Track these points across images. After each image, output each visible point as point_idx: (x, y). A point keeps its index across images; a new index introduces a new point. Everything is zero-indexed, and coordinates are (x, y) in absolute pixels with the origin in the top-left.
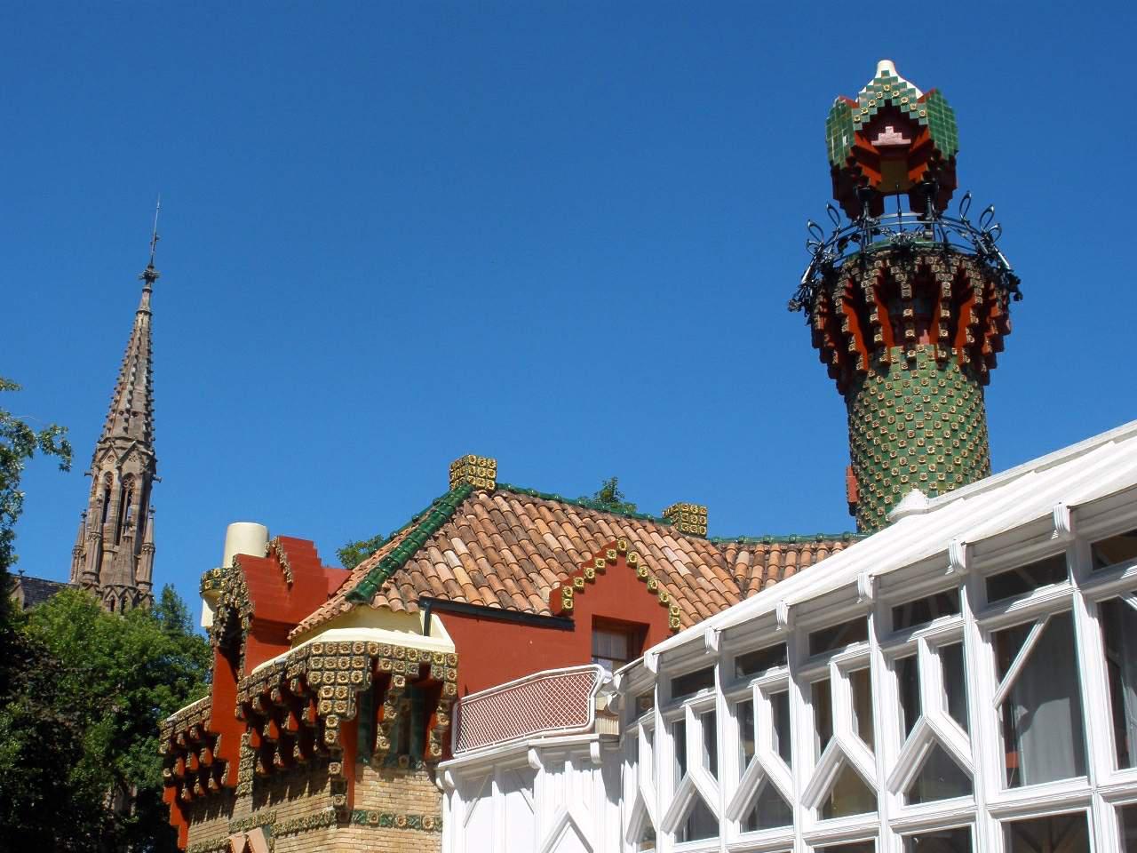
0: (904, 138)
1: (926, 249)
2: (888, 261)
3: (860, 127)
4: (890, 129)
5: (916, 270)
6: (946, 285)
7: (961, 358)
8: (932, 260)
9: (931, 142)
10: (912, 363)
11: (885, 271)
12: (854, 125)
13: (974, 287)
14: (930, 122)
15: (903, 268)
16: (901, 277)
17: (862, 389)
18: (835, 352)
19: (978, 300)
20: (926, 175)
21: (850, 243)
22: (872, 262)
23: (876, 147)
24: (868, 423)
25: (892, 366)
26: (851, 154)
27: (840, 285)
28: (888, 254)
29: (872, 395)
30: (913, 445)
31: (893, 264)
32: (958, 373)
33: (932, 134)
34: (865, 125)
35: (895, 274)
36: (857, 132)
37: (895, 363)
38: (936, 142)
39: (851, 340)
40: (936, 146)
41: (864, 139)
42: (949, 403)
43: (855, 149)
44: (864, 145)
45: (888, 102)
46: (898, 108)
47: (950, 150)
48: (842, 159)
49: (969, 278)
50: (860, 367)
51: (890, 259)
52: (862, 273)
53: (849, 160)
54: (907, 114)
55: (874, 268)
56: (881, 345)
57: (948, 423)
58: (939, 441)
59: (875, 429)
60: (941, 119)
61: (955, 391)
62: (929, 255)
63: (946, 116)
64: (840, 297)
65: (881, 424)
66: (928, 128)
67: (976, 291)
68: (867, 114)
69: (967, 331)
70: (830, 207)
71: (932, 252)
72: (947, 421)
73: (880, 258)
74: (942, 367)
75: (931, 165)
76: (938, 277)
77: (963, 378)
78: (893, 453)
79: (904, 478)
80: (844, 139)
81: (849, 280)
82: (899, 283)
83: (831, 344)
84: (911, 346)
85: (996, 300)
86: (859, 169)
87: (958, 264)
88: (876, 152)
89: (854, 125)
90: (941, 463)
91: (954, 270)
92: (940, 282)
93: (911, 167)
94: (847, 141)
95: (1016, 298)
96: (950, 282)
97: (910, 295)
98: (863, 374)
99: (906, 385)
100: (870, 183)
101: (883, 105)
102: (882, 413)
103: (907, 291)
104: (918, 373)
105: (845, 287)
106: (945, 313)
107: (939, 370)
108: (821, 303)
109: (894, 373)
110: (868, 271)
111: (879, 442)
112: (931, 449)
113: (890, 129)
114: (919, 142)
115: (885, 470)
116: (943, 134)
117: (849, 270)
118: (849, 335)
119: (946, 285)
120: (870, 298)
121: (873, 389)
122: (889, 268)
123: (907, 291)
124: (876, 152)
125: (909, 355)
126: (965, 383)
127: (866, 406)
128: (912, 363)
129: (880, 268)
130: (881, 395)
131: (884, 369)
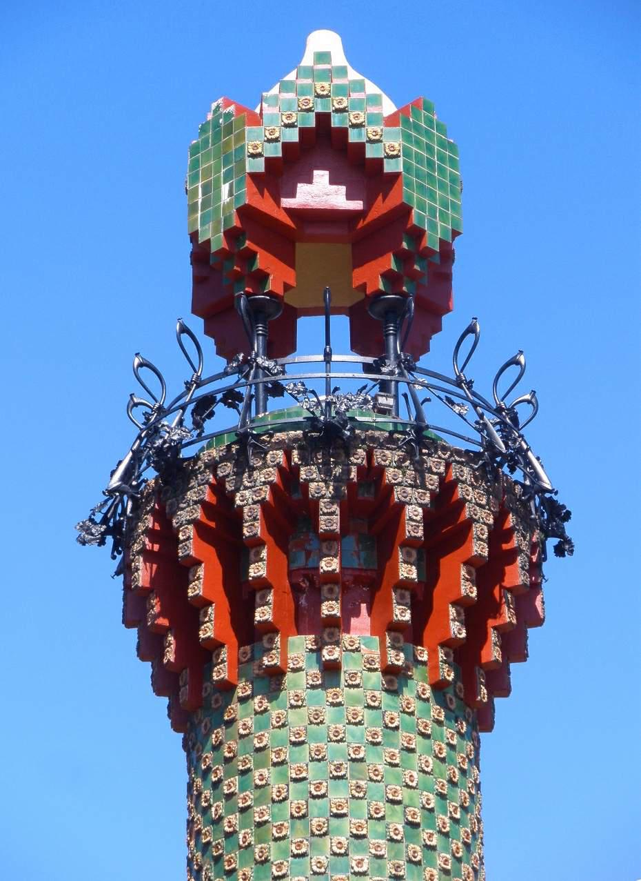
0: (350, 197)
1: (377, 434)
2: (295, 452)
3: (259, 166)
4: (321, 177)
5: (353, 475)
6: (414, 512)
7: (435, 668)
8: (388, 457)
9: (405, 210)
10: (331, 671)
11: (289, 474)
12: (248, 161)
13: (470, 522)
14: (407, 168)
15: (326, 470)
16: (319, 487)
18: (171, 639)
19: (479, 548)
20: (388, 276)
21: (220, 408)
22: (261, 452)
23: (290, 212)
24: (229, 796)
25: (289, 676)
26: (235, 222)
27: (191, 495)
28: (296, 440)
29: (242, 736)
30: (321, 853)
31: (305, 461)
32: (427, 700)
33: (410, 193)
35: (308, 481)
36: (254, 176)
38: (415, 210)
39: (206, 614)
40: (414, 220)
41: (266, 193)
42: (406, 765)
43: (246, 212)
44: (265, 205)
47: (444, 228)
48: (216, 231)
49: (463, 502)
50: (221, 673)
51: (300, 448)
52: (239, 474)
53: (232, 235)
54: (361, 147)
55: (265, 466)
56: (270, 629)
58: (378, 847)
59: (243, 810)
60: (430, 164)
61: (420, 738)
62: (382, 446)
63: (441, 159)
64: (189, 522)
65: (258, 801)
66: (403, 179)
67: (476, 529)
68: (276, 140)
69: (452, 612)
70: (184, 329)
73: (279, 445)
74: (396, 687)
75: (403, 258)
76: (397, 494)
77: (436, 711)
78: (279, 866)
80: (225, 188)
81: (211, 486)
82: (316, 502)
83: (164, 622)
84: (331, 635)
85: (516, 552)
86: (251, 256)
87: (442, 469)
88: (288, 221)
89: (248, 161)
91: (433, 481)
92: (401, 506)
93: (359, 261)
94: (231, 194)
95: (559, 551)
96: (420, 505)
97: (336, 527)
98: (227, 688)
100: (270, 287)
101: (312, 123)
102: (262, 777)
103: (330, 519)
104: (344, 694)
105: (202, 503)
106: (407, 572)
107: (386, 691)
108: (148, 532)
109: (292, 692)
110: (252, 469)
111: (251, 839)
112: (360, 863)
113: (321, 177)
114: (381, 207)
116: (432, 196)
117: (213, 466)
119: (414, 512)
120: (253, 527)
122: (297, 468)
123: (330, 519)
124: (288, 221)
125: (326, 655)
126: (439, 723)
127: (228, 760)
128: (331, 671)
129: (278, 466)
130: (260, 738)
131: (272, 680)
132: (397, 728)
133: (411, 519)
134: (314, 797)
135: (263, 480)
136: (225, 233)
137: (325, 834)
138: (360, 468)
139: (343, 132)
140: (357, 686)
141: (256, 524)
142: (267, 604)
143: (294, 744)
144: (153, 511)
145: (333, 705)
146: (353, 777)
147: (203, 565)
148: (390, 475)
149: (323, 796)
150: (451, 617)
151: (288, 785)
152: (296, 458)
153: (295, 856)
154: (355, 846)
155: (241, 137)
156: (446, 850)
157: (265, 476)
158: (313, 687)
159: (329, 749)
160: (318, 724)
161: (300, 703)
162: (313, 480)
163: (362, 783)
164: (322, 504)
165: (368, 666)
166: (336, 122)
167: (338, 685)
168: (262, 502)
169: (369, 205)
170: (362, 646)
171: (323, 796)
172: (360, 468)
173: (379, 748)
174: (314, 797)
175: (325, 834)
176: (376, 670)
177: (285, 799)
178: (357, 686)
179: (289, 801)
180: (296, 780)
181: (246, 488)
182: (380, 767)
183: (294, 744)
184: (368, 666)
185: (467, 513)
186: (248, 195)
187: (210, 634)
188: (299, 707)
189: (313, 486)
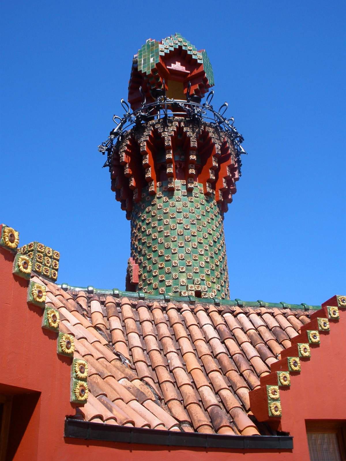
0: (186, 70)
3: (163, 54)
7: (218, 196)
8: (211, 130)
9: (203, 73)
10: (190, 191)
11: (180, 129)
17: (150, 205)
18: (133, 179)
22: (171, 122)
23: (169, 69)
24: (154, 228)
25: (176, 191)
26: (155, 67)
27: (145, 134)
28: (182, 120)
29: (158, 209)
30: (189, 247)
31: (186, 126)
35: (187, 132)
36: (161, 56)
37: (178, 190)
43: (158, 65)
44: (164, 65)
45: (180, 47)
46: (186, 51)
48: (149, 69)
53: (153, 70)
54: (191, 56)
55: (172, 126)
56: (171, 175)
59: (160, 232)
64: (144, 141)
65: (165, 229)
69: (224, 180)
71: (210, 126)
73: (177, 120)
78: (175, 250)
79: (182, 268)
80: (152, 60)
81: (152, 131)
84: (191, 180)
88: (167, 70)
92: (214, 144)
99: (185, 206)
103: (194, 144)
105: (149, 135)
106: (214, 164)
107: (206, 200)
108: (127, 145)
109: (158, 205)
110: (168, 126)
114: (196, 72)
115: (167, 261)
118: (147, 166)
120: (168, 143)
121: (159, 203)
122: (183, 127)
125: (189, 186)
127: (153, 216)
128: (190, 191)
129: (176, 126)
130: (166, 210)
131: (170, 192)
134: (186, 229)
135: (171, 130)
136: (151, 70)
137: (190, 241)
140: (197, 197)
141: (170, 142)
142: (171, 167)
143: (178, 212)
144: (129, 139)
145: (190, 202)
146: (198, 225)
147: (148, 155)
148: (210, 134)
149: (188, 229)
150: (224, 182)
151: (176, 225)
152: (182, 124)
153: (180, 247)
154: (199, 246)
155: (158, 46)
157: (172, 129)
158: (184, 196)
159: (189, 215)
160: (186, 207)
161: (180, 200)
162: (188, 132)
163: (201, 227)
164: (191, 138)
165: (200, 192)
166: (184, 48)
167: (192, 196)
168: (171, 136)
170: (198, 186)
171: (188, 229)
173: (205, 217)
174: (186, 229)
175: (190, 241)
176: (202, 193)
177: (176, 229)
178: (197, 197)
179: (177, 230)
180: (179, 223)
181: (166, 132)
182: (205, 223)
183: (178, 212)
184: (200, 192)
186: (159, 60)
187: (150, 176)
188: (180, 201)
189: (188, 133)
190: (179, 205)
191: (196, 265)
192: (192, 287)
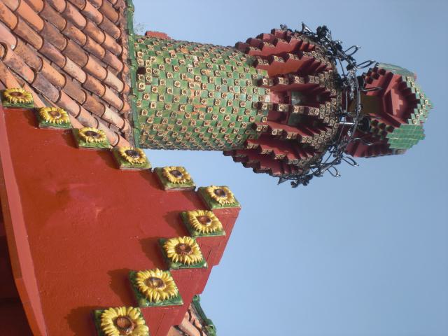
0: (397, 110)
3: (404, 80)
4: (401, 102)
9: (398, 125)
10: (259, 83)
11: (324, 69)
16: (324, 77)
20: (375, 123)
26: (387, 72)
34: (405, 84)
35: (324, 74)
40: (396, 129)
44: (393, 83)
57: (213, 103)
67: (311, 138)
72: (214, 104)
75: (383, 126)
76: (323, 106)
77: (246, 124)
85: (299, 158)
90: (181, 93)
91: (327, 120)
92: (319, 107)
95: (292, 183)
103: (313, 80)
104: (251, 87)
124: (387, 91)
129: (327, 65)
132: (240, 106)
133: (315, 110)
138: (329, 93)
139: (416, 107)
145: (247, 83)
156: (197, 124)
158: (252, 76)
166: (419, 105)
169: (396, 116)
172: (329, 93)
178: (254, 92)
185: (315, 134)
190: (240, 69)
191: (175, 77)
192: (148, 63)
